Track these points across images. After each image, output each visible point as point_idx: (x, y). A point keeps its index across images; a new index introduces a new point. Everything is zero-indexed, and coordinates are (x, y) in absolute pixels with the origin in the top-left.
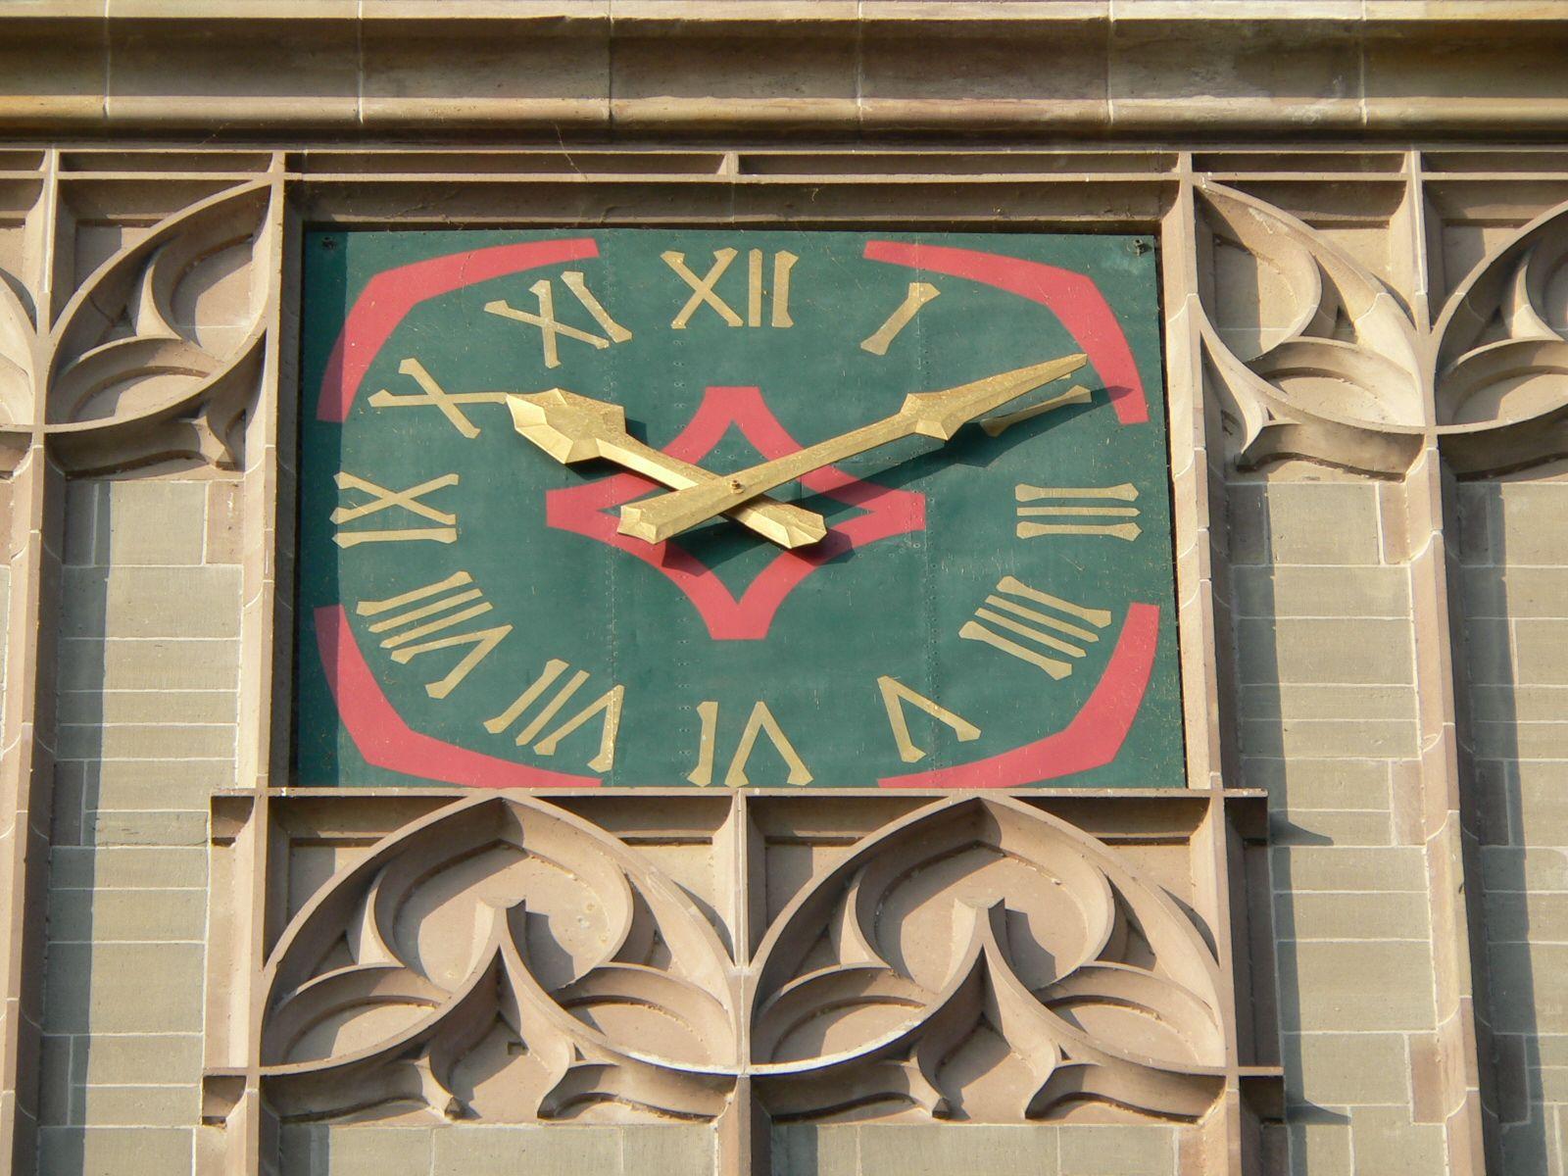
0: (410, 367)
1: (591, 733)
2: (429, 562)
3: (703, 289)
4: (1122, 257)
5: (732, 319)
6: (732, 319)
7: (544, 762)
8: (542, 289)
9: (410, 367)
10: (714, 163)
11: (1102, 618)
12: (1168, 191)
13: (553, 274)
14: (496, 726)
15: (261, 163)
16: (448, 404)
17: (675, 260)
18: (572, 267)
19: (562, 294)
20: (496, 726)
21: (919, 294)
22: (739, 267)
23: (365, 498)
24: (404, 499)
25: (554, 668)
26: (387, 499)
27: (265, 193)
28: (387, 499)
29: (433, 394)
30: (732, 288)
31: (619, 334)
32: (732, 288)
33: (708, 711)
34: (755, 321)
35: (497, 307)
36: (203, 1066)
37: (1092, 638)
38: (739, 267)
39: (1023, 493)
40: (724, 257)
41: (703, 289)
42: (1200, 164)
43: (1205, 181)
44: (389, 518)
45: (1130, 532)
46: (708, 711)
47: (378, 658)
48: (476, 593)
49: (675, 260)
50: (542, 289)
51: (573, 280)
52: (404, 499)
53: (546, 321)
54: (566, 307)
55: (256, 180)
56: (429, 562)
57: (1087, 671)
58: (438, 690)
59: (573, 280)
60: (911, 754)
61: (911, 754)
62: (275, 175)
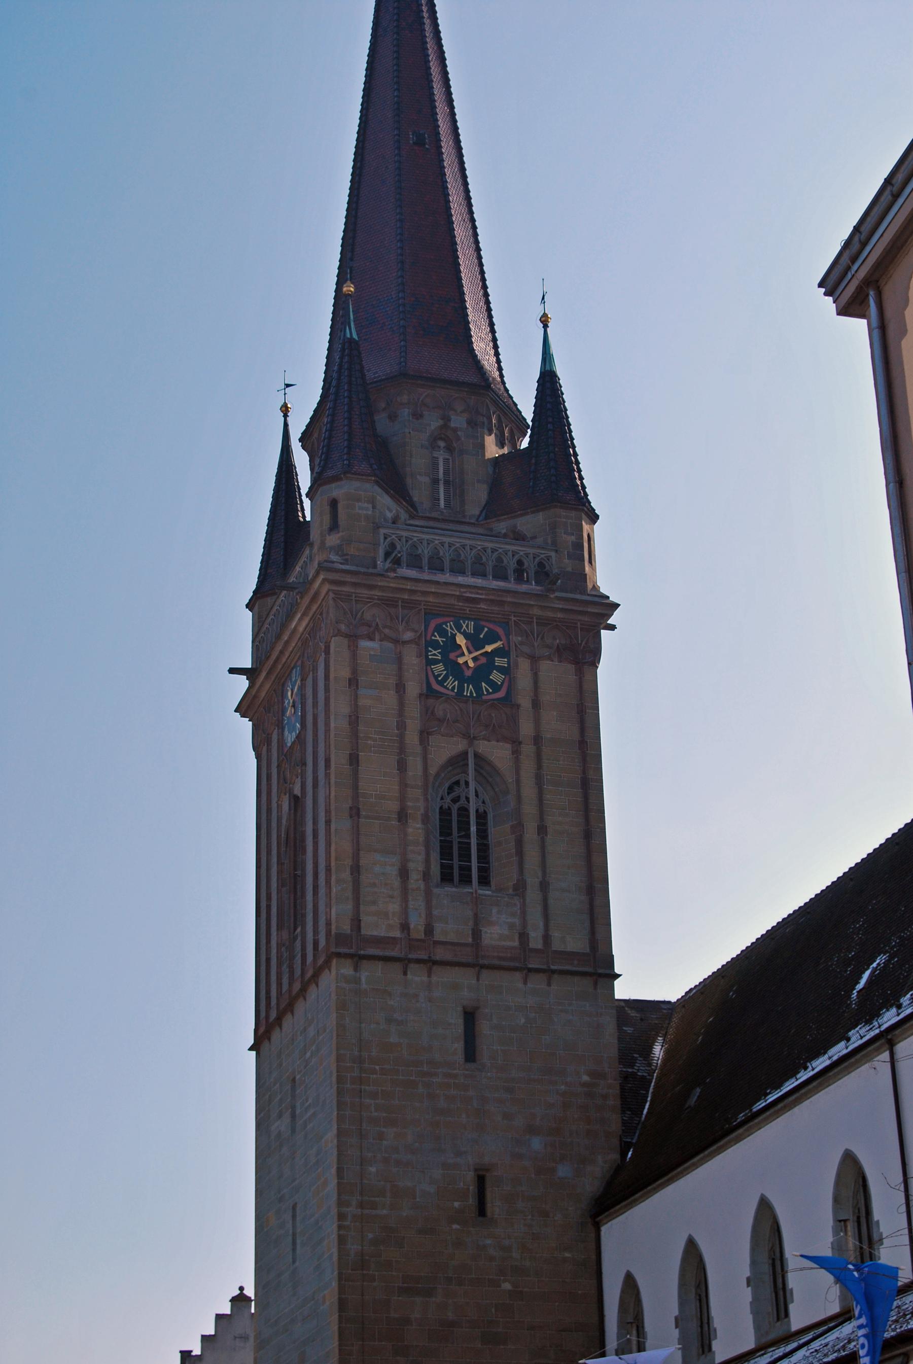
0: (436, 634)
11: (503, 677)
16: (438, 638)
17: (461, 621)
18: (452, 621)
20: (445, 684)
21: (486, 629)
22: (468, 624)
23: (432, 652)
26: (434, 652)
28: (434, 652)
29: (438, 638)
30: (467, 626)
32: (467, 626)
33: (466, 685)
38: (468, 624)
42: (514, 616)
43: (515, 619)
44: (434, 655)
46: (466, 685)
47: (433, 673)
51: (451, 623)
53: (449, 629)
54: (451, 628)
57: (502, 683)
58: (440, 679)
59: (451, 623)
60: (485, 693)
61: (485, 693)
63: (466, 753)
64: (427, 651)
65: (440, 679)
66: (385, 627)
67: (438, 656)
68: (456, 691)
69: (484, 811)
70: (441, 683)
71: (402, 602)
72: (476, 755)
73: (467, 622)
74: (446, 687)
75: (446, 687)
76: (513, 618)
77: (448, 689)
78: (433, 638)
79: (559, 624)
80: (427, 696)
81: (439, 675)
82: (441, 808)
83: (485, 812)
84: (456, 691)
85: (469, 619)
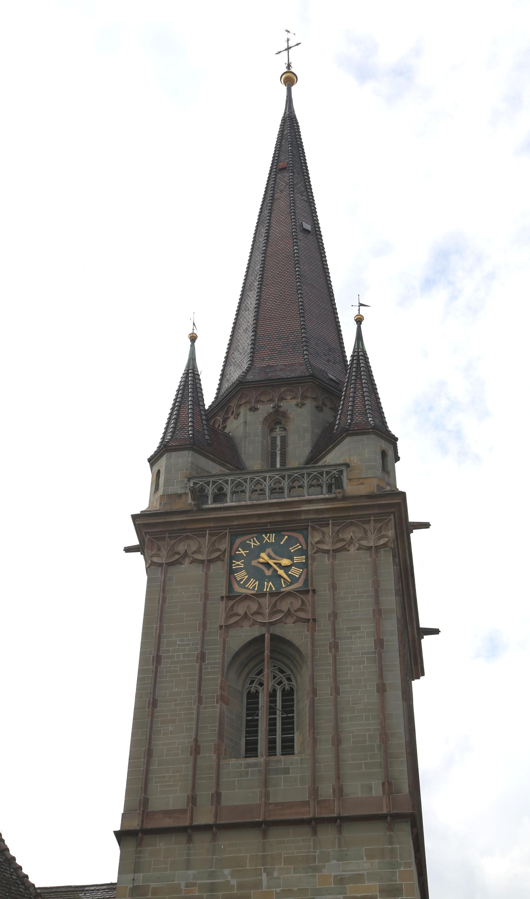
0: (240, 549)
1: (255, 587)
2: (241, 569)
3: (266, 538)
4: (305, 532)
5: (269, 542)
6: (269, 542)
7: (251, 589)
8: (252, 540)
9: (240, 549)
10: (267, 526)
11: (301, 570)
12: (308, 525)
13: (253, 538)
14: (247, 586)
15: (226, 529)
16: (243, 552)
17: (264, 535)
18: (254, 537)
19: (253, 540)
20: (247, 586)
21: (286, 537)
22: (270, 536)
24: (239, 563)
25: (252, 579)
26: (237, 563)
27: (227, 532)
28: (237, 563)
30: (269, 538)
31: (259, 544)
32: (269, 538)
34: (271, 541)
35: (248, 542)
36: (220, 624)
37: (300, 572)
39: (295, 558)
40: (268, 535)
41: (266, 538)
42: (311, 522)
43: (311, 524)
45: (304, 561)
46: (266, 583)
48: (245, 572)
49: (264, 535)
50: (252, 540)
52: (239, 563)
55: (226, 531)
56: (241, 569)
57: (300, 576)
58: (241, 583)
59: (255, 538)
61: (284, 586)
62: (228, 531)
63: (261, 638)
64: (231, 563)
65: (241, 583)
66: (195, 552)
67: (242, 565)
68: (256, 589)
69: (291, 688)
70: (243, 586)
71: (209, 531)
72: (274, 638)
73: (268, 535)
74: (247, 588)
75: (247, 588)
76: (310, 524)
77: (249, 589)
78: (237, 552)
79: (353, 520)
80: (229, 598)
81: (241, 580)
82: (249, 693)
83: (292, 690)
84: (256, 589)
85: (270, 533)
